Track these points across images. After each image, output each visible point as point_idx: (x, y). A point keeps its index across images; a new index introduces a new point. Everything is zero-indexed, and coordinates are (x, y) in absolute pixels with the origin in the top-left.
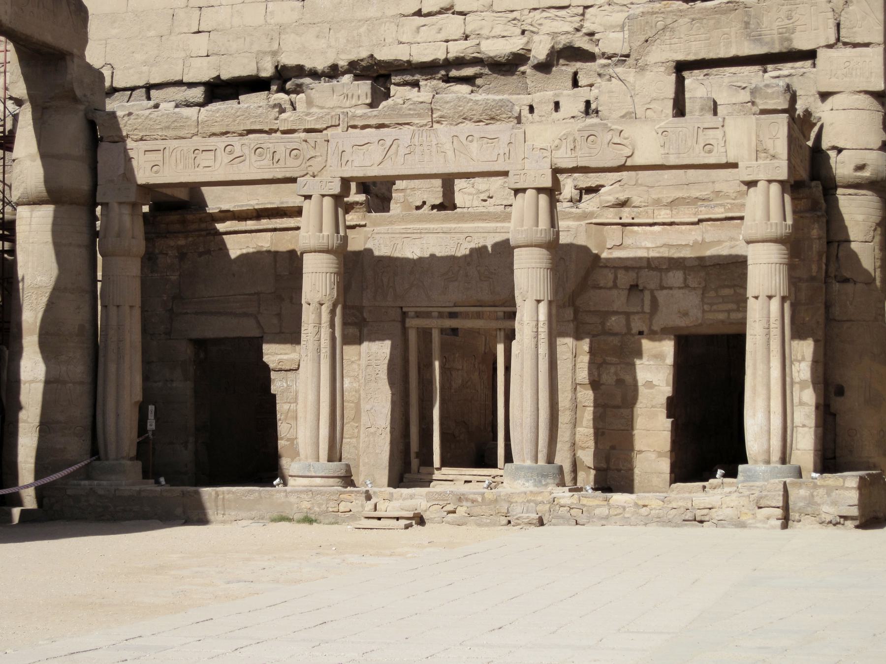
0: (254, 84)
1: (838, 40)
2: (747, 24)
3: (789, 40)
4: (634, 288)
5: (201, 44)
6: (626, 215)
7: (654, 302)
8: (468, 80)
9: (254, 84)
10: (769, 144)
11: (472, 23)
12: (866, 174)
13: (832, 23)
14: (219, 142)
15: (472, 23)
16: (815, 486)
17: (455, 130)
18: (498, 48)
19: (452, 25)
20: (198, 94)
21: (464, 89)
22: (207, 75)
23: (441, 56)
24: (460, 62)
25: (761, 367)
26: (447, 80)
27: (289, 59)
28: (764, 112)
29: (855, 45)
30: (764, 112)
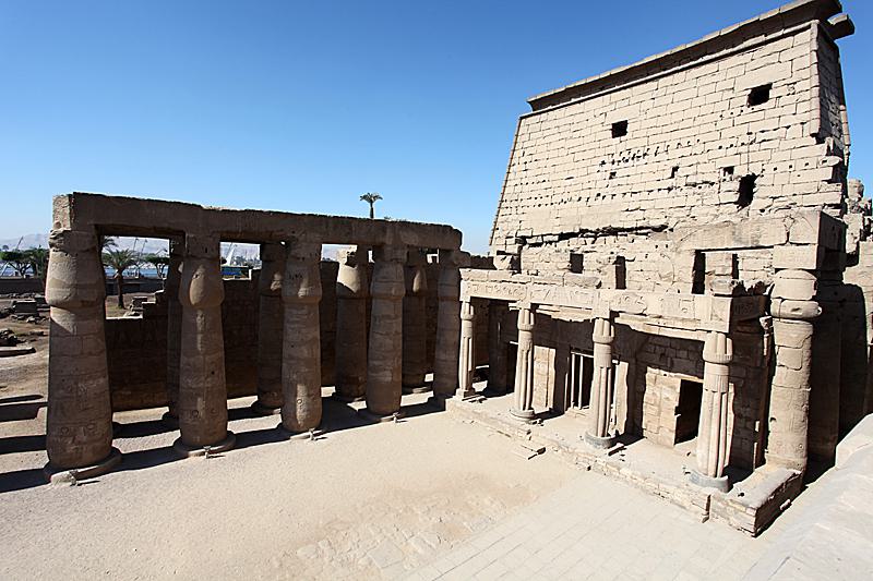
0: (573, 235)
1: (787, 241)
2: (734, 233)
3: (757, 241)
4: (662, 355)
5: (558, 222)
6: (661, 321)
7: (672, 362)
8: (646, 234)
9: (573, 235)
10: (719, 313)
11: (647, 214)
12: (799, 313)
13: (784, 233)
14: (494, 284)
15: (647, 214)
16: (728, 505)
17: (571, 289)
18: (657, 224)
19: (640, 214)
20: (556, 238)
21: (645, 237)
23: (634, 226)
24: (641, 228)
25: (707, 427)
26: (637, 234)
28: (716, 295)
29: (798, 244)
30: (716, 295)
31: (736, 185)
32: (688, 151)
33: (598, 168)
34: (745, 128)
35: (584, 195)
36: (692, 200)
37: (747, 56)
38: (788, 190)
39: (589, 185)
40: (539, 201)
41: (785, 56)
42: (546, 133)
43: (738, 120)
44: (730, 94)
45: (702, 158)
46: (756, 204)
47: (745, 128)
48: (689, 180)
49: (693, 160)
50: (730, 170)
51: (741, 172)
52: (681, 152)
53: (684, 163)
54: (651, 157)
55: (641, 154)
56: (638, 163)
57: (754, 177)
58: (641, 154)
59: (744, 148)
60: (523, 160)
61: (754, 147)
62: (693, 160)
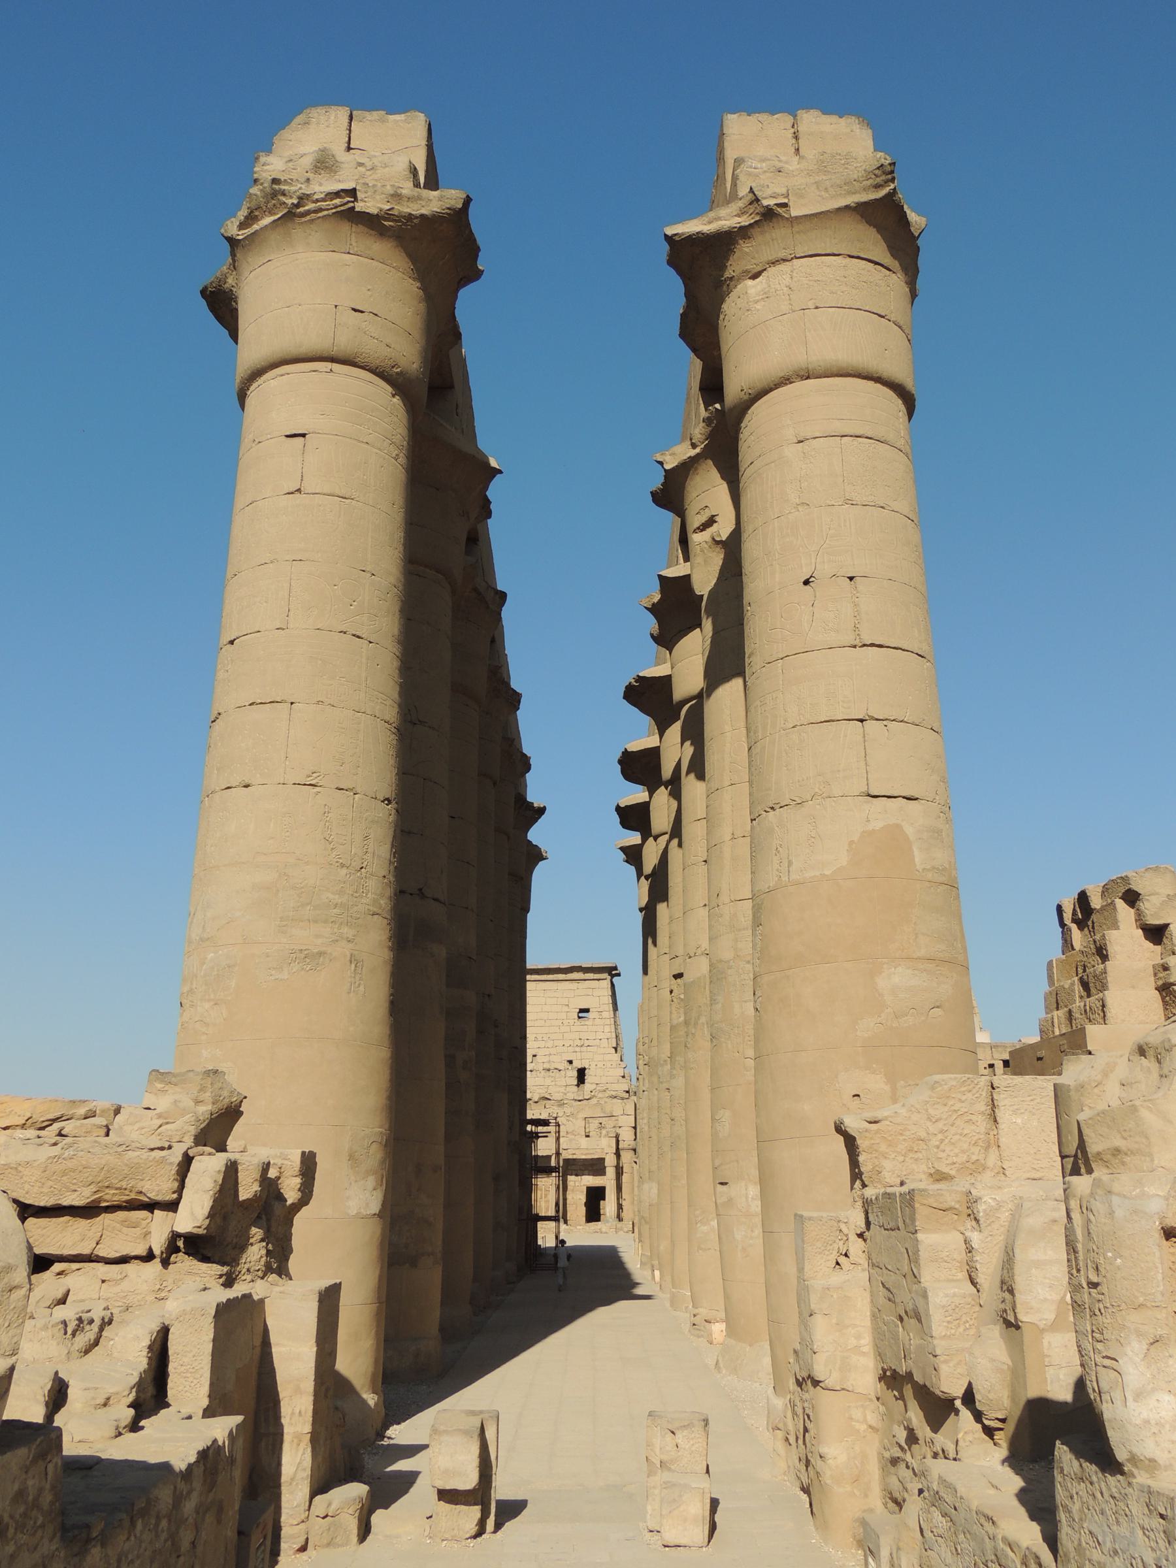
31: (575, 1074)
32: (542, 1044)
34: (576, 1036)
36: (548, 1081)
37: (574, 985)
38: (604, 1080)
41: (596, 993)
43: (574, 1028)
44: (566, 1009)
45: (553, 1051)
46: (588, 1086)
47: (576, 1036)
48: (547, 1066)
50: (571, 1062)
51: (578, 1064)
53: (540, 1053)
57: (584, 1069)
59: (578, 1049)
61: (584, 1049)
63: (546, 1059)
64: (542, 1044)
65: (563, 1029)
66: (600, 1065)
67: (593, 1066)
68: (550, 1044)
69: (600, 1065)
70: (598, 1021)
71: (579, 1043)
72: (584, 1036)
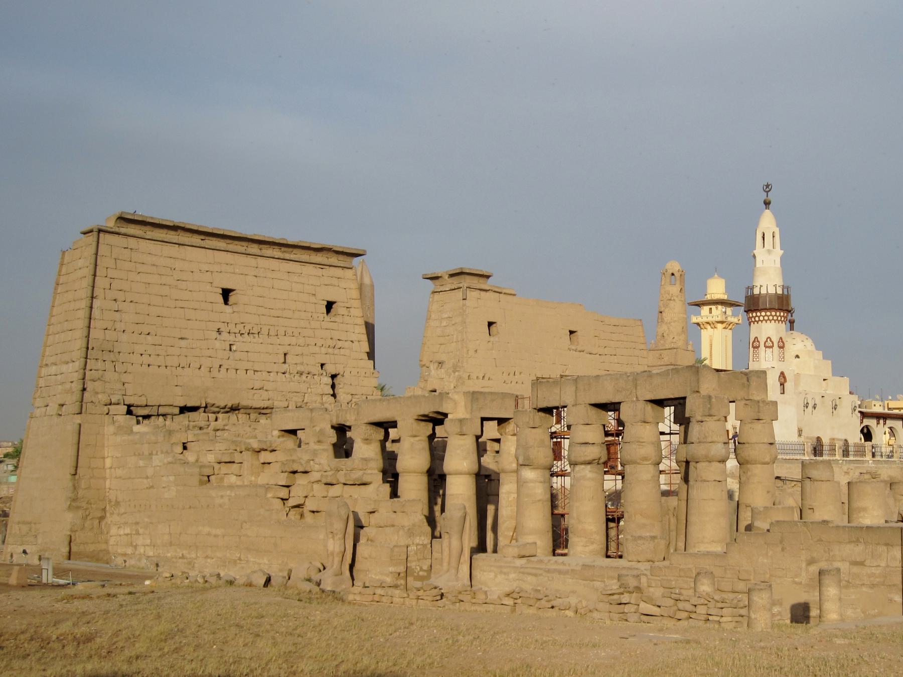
5: (178, 391)
19: (265, 395)
20: (177, 411)
22: (182, 405)
27: (210, 401)
32: (293, 341)
33: (215, 334)
35: (206, 363)
37: (317, 271)
39: (209, 353)
40: (146, 359)
41: (343, 284)
42: (141, 268)
48: (300, 368)
49: (299, 350)
51: (331, 369)
52: (287, 340)
54: (263, 338)
55: (255, 331)
56: (253, 340)
58: (255, 331)
59: (330, 350)
60: (111, 294)
61: (336, 351)
62: (299, 350)
63: (298, 360)
64: (293, 341)
65: (314, 324)
66: (354, 372)
67: (347, 374)
68: (301, 341)
69: (354, 372)
70: (347, 319)
71: (332, 343)
72: (336, 335)
